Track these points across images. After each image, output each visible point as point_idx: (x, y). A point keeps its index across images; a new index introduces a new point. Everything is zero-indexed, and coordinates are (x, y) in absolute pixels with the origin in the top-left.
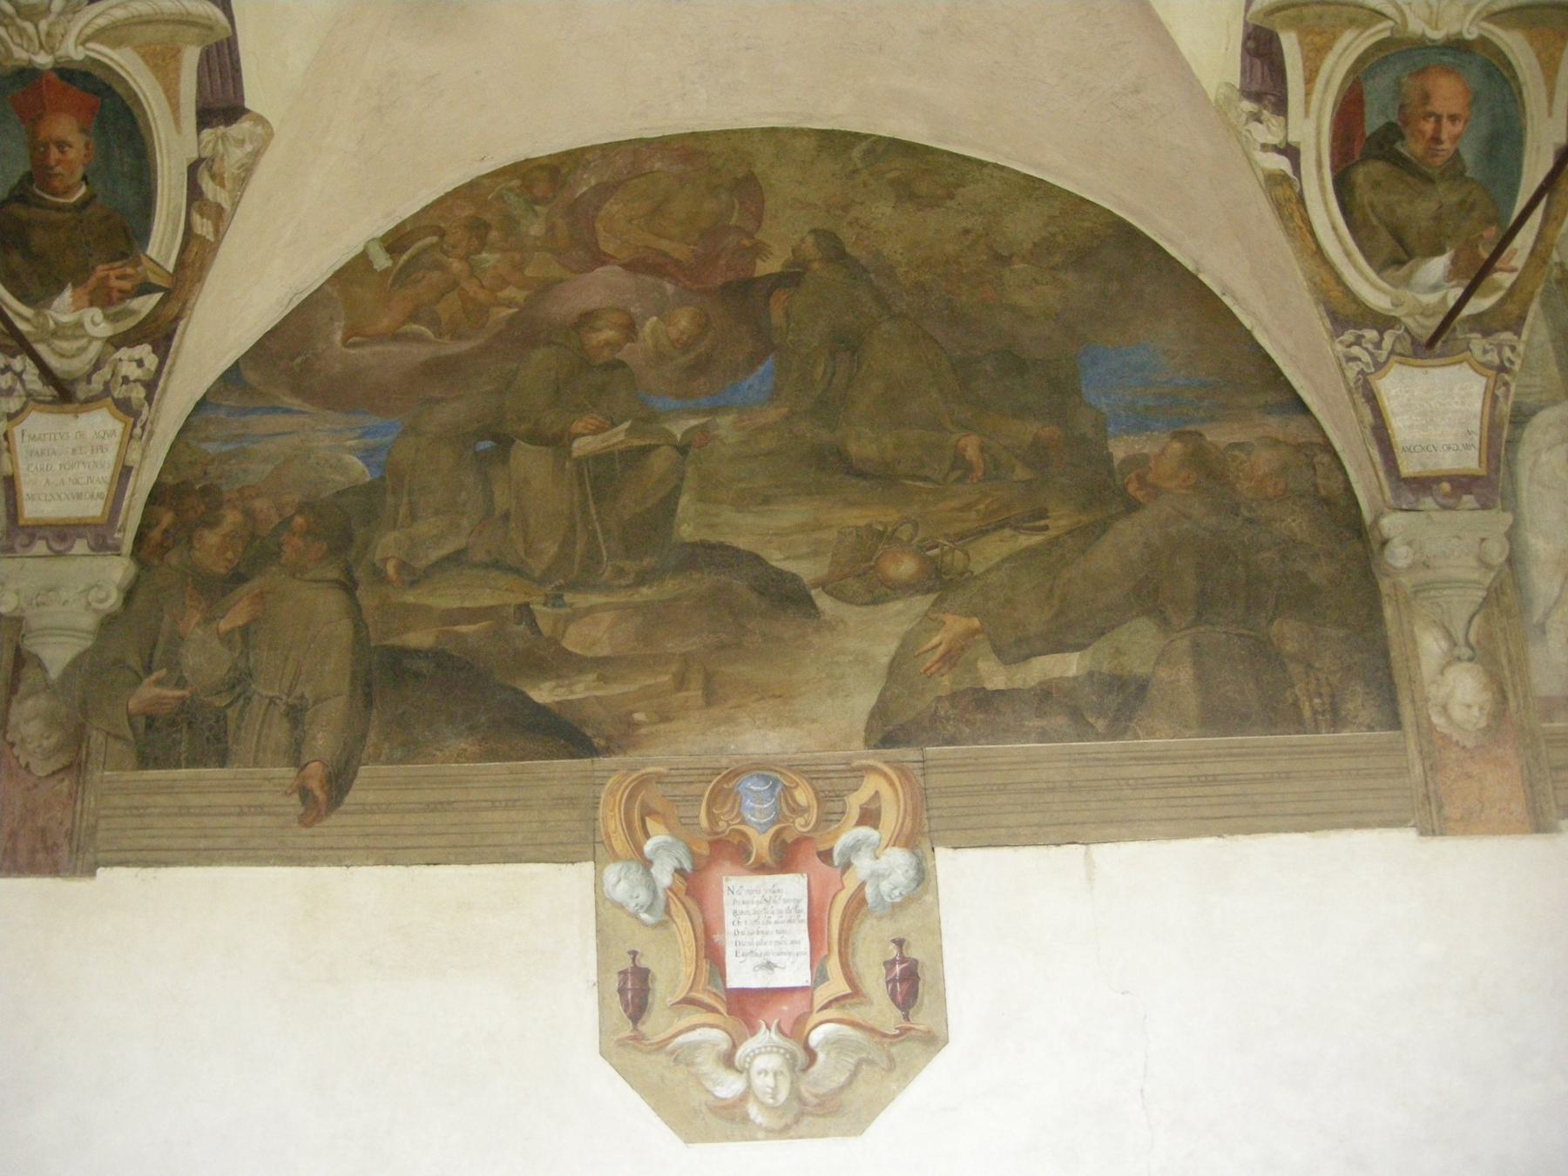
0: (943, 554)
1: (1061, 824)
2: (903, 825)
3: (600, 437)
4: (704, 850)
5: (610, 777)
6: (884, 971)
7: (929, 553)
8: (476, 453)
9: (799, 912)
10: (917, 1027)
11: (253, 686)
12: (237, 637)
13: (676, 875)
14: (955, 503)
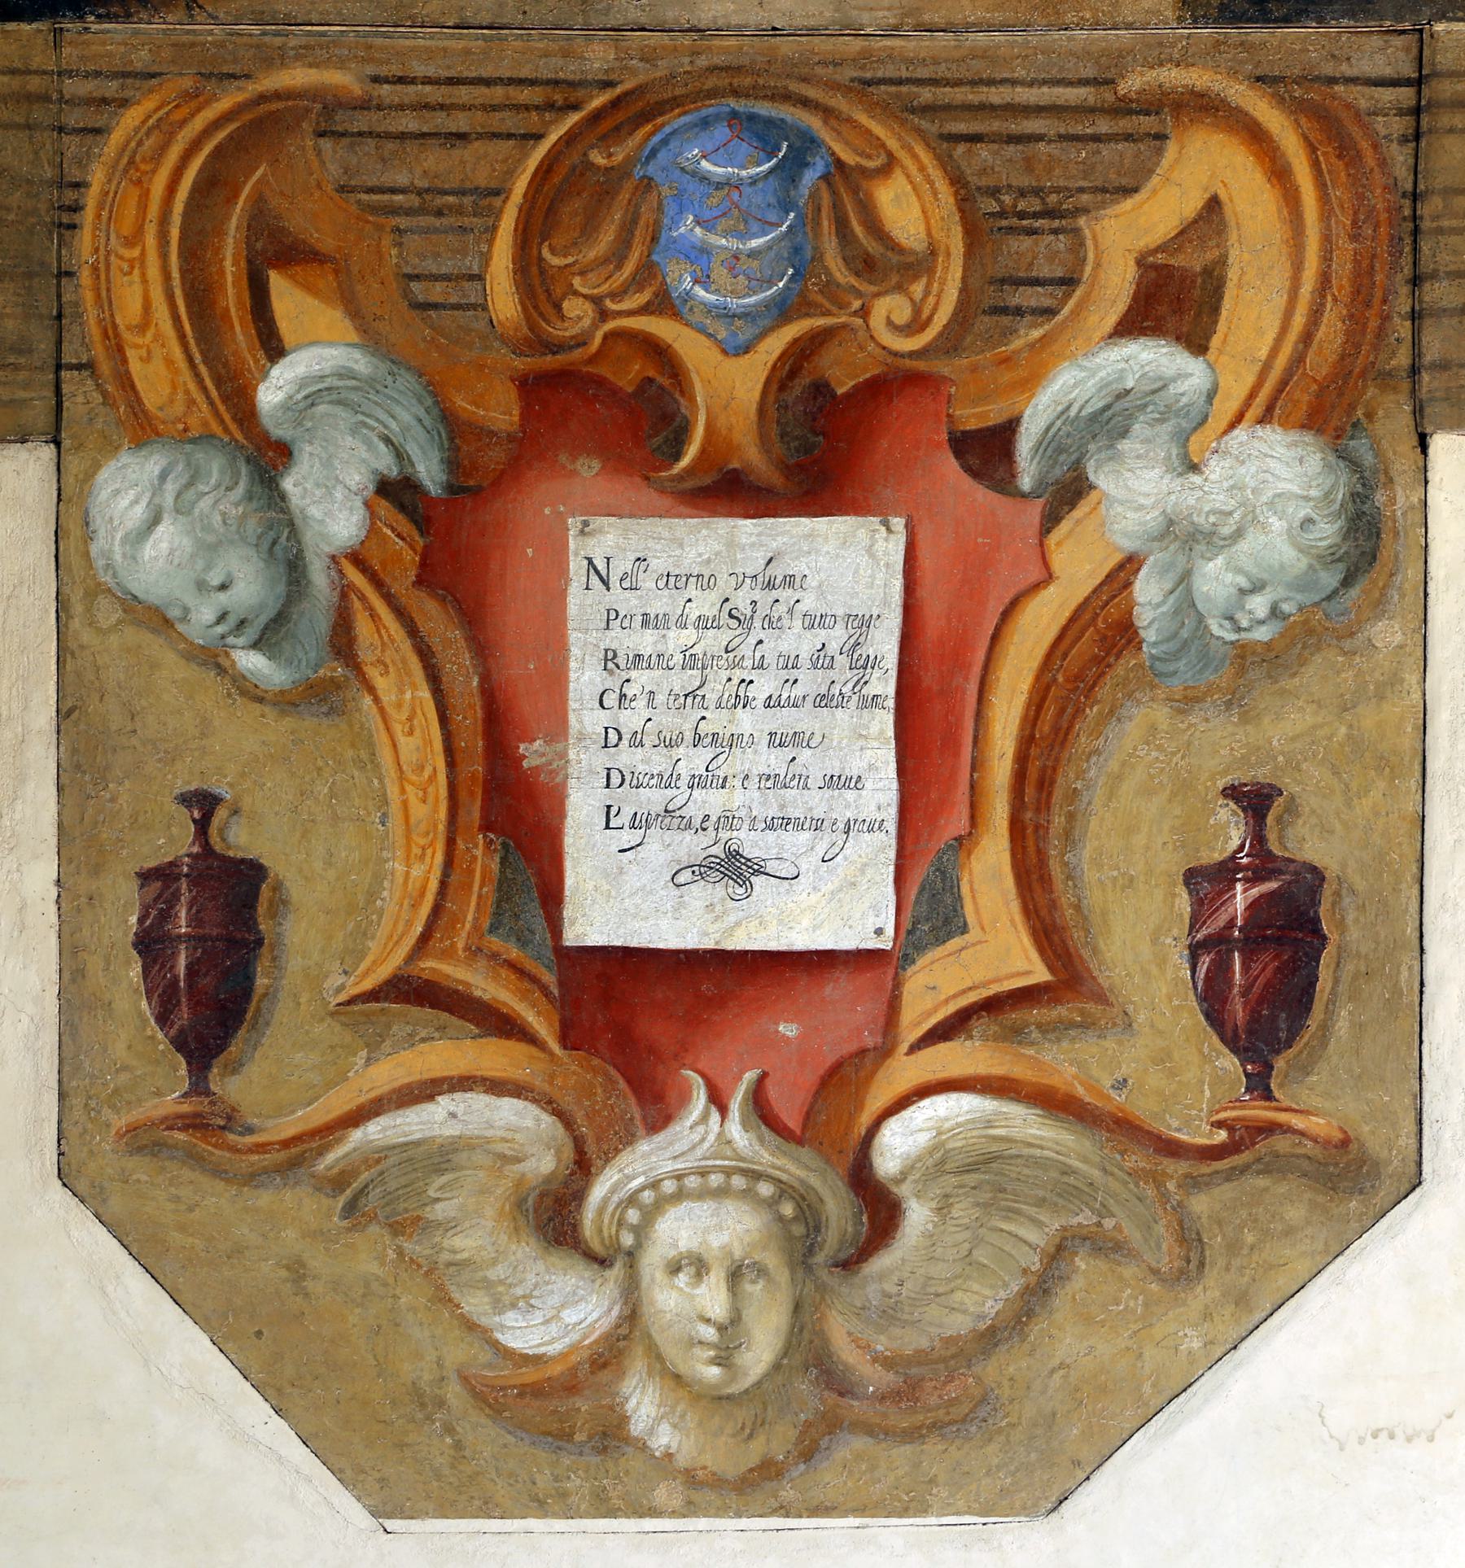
2: (1307, 337)
5: (124, 103)
6: (1184, 903)
9: (870, 663)
10: (1297, 1122)
13: (384, 507)
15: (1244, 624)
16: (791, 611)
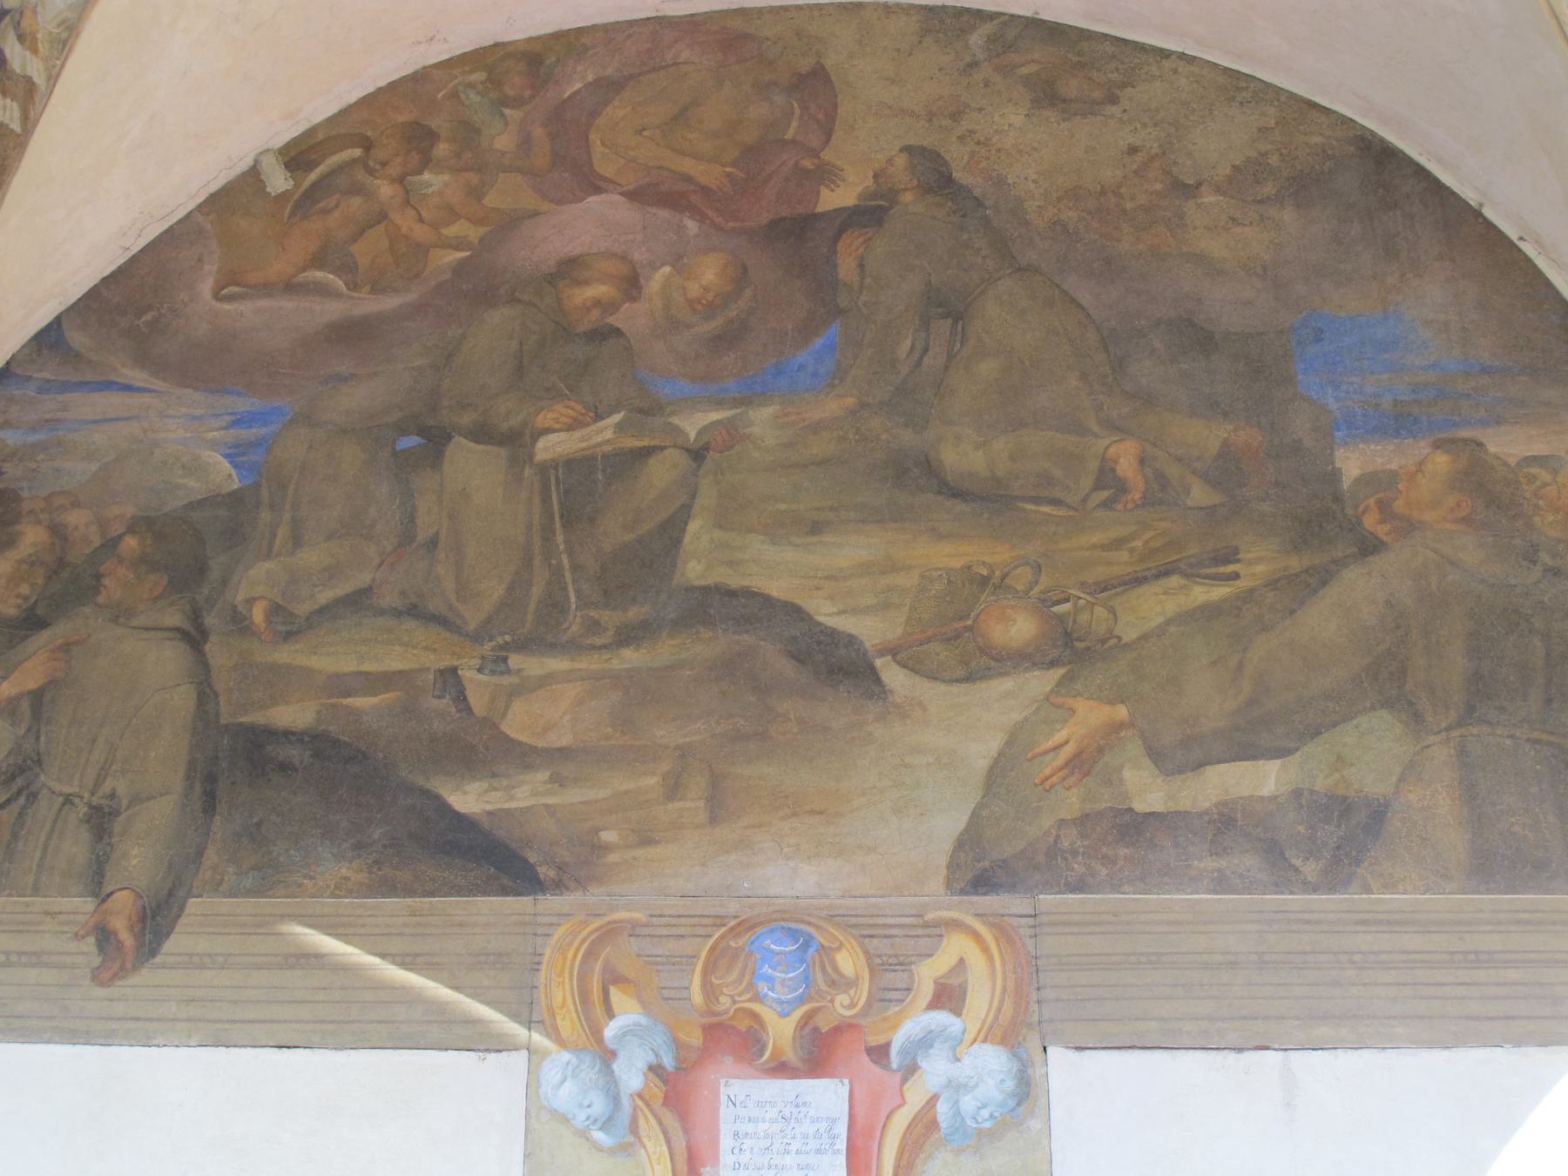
0: (1077, 610)
1: (1244, 1018)
2: (999, 1010)
3: (577, 434)
4: (695, 1039)
5: (559, 925)
7: (1055, 609)
8: (395, 454)
11: (42, 777)
12: (25, 706)
13: (651, 1075)
14: (1098, 538)
15: (980, 1121)
16: (805, 1116)
